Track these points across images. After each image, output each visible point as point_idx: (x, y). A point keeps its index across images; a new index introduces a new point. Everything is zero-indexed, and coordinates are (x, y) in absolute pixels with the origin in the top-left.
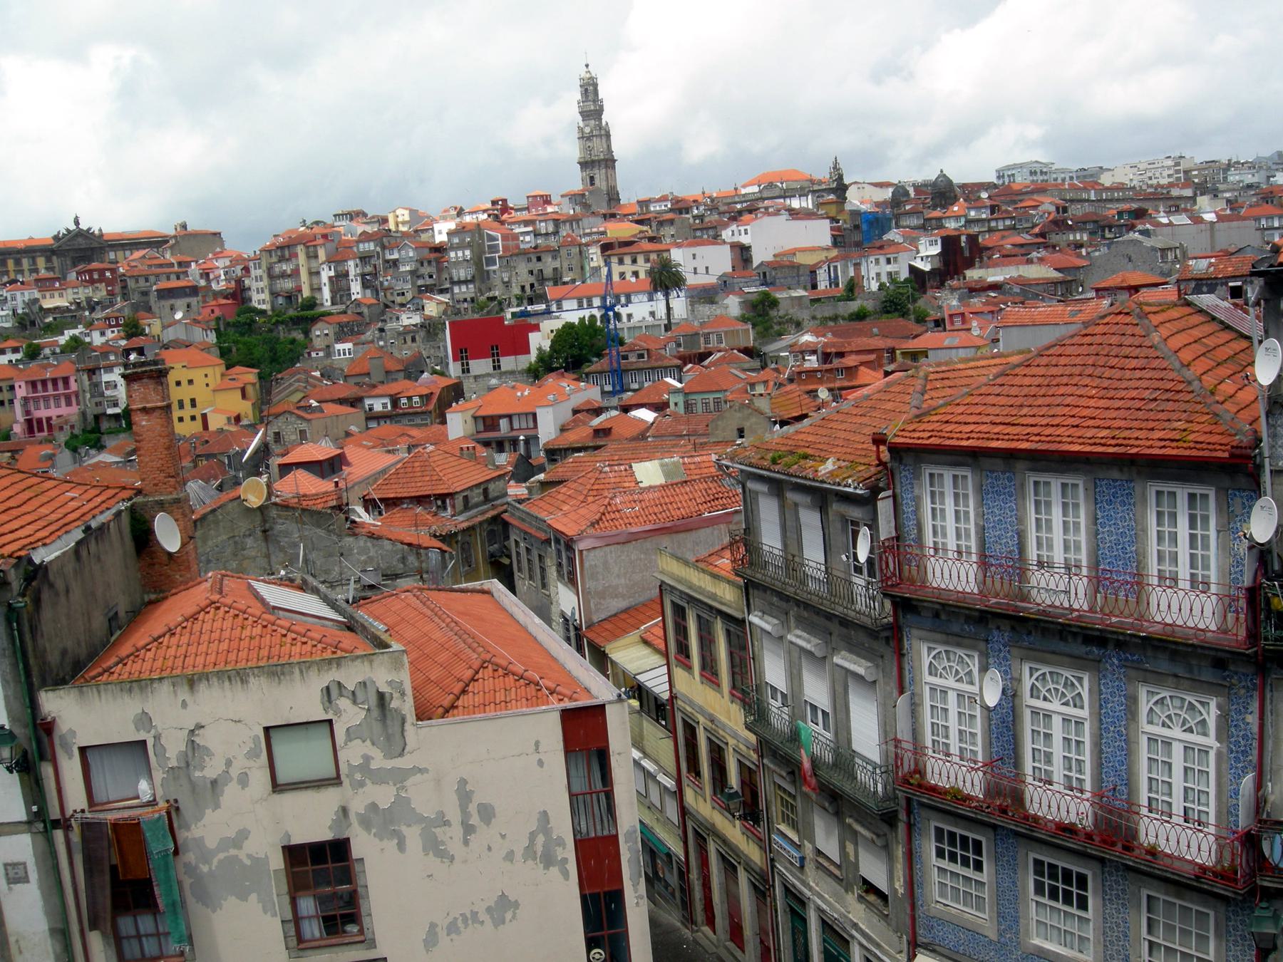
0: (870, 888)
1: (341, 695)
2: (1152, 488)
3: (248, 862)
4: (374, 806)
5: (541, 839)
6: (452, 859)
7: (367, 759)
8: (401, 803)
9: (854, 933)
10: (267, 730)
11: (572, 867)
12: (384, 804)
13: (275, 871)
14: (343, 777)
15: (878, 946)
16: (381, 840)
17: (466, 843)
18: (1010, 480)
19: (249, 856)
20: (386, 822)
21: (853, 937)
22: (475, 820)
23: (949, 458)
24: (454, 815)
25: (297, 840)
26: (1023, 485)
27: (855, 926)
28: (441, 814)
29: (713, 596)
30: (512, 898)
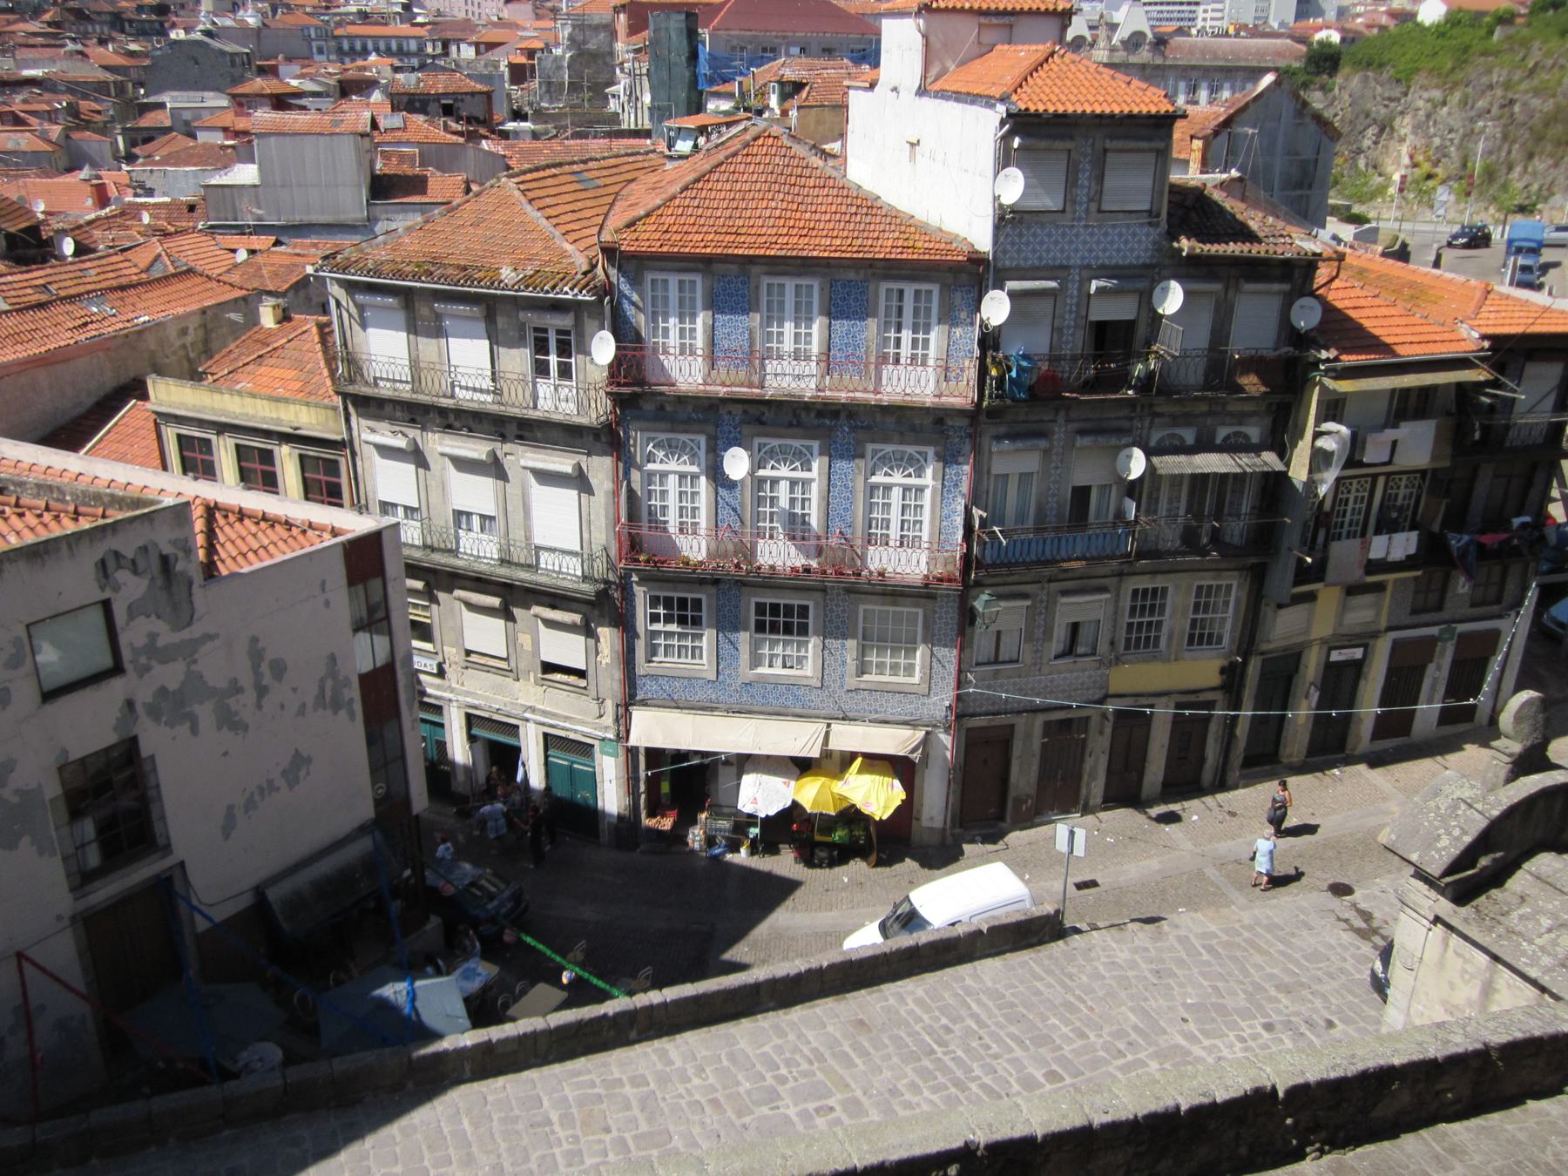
0: (549, 668)
1: (119, 567)
2: (884, 286)
3: (15, 800)
4: (163, 691)
5: (329, 684)
6: (246, 728)
7: (153, 637)
8: (194, 680)
9: (527, 715)
10: (28, 626)
11: (358, 707)
12: (173, 685)
13: (52, 800)
14: (127, 666)
15: (567, 718)
16: (172, 727)
17: (259, 707)
18: (743, 283)
19: (17, 792)
20: (173, 707)
21: (527, 720)
22: (267, 679)
23: (678, 265)
24: (246, 680)
25: (75, 754)
26: (757, 287)
27: (533, 709)
28: (235, 681)
29: (279, 421)
30: (305, 755)
